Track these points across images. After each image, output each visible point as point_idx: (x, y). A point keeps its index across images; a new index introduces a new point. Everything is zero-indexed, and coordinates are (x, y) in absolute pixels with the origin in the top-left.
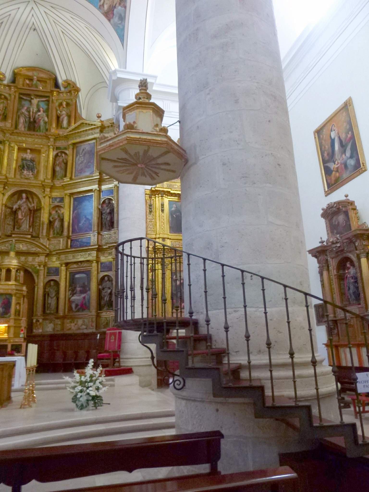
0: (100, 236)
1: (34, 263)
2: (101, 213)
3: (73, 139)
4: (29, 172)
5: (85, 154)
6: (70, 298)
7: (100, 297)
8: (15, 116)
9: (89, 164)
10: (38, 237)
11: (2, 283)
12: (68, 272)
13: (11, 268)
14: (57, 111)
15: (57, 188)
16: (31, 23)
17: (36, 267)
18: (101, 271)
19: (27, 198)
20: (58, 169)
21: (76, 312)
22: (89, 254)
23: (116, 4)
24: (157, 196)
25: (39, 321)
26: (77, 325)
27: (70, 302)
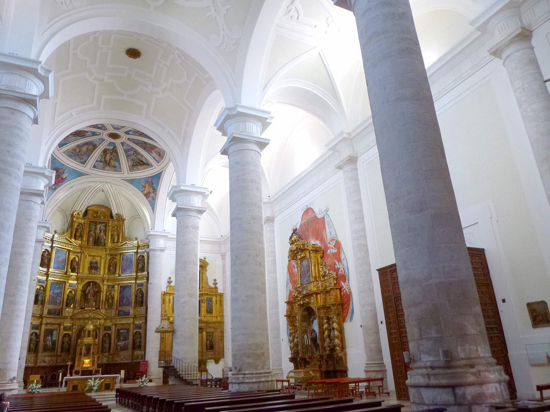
1: (97, 324)
2: (136, 297)
5: (127, 260)
7: (134, 344)
10: (98, 308)
12: (116, 329)
14: (111, 232)
20: (111, 268)
21: (120, 351)
22: (129, 320)
27: (117, 346)
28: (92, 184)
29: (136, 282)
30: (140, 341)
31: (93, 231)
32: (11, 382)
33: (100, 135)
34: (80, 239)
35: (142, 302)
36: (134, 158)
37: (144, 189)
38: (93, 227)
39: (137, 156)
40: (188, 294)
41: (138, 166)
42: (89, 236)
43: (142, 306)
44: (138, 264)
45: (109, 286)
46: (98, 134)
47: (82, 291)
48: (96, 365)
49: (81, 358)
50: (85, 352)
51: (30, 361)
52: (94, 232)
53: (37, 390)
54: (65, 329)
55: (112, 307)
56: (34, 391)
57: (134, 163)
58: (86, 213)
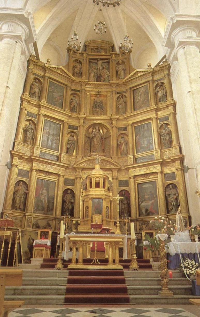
4: (100, 110)
5: (140, 95)
8: (87, 74)
26: (148, 227)
35: (171, 142)
45: (119, 129)
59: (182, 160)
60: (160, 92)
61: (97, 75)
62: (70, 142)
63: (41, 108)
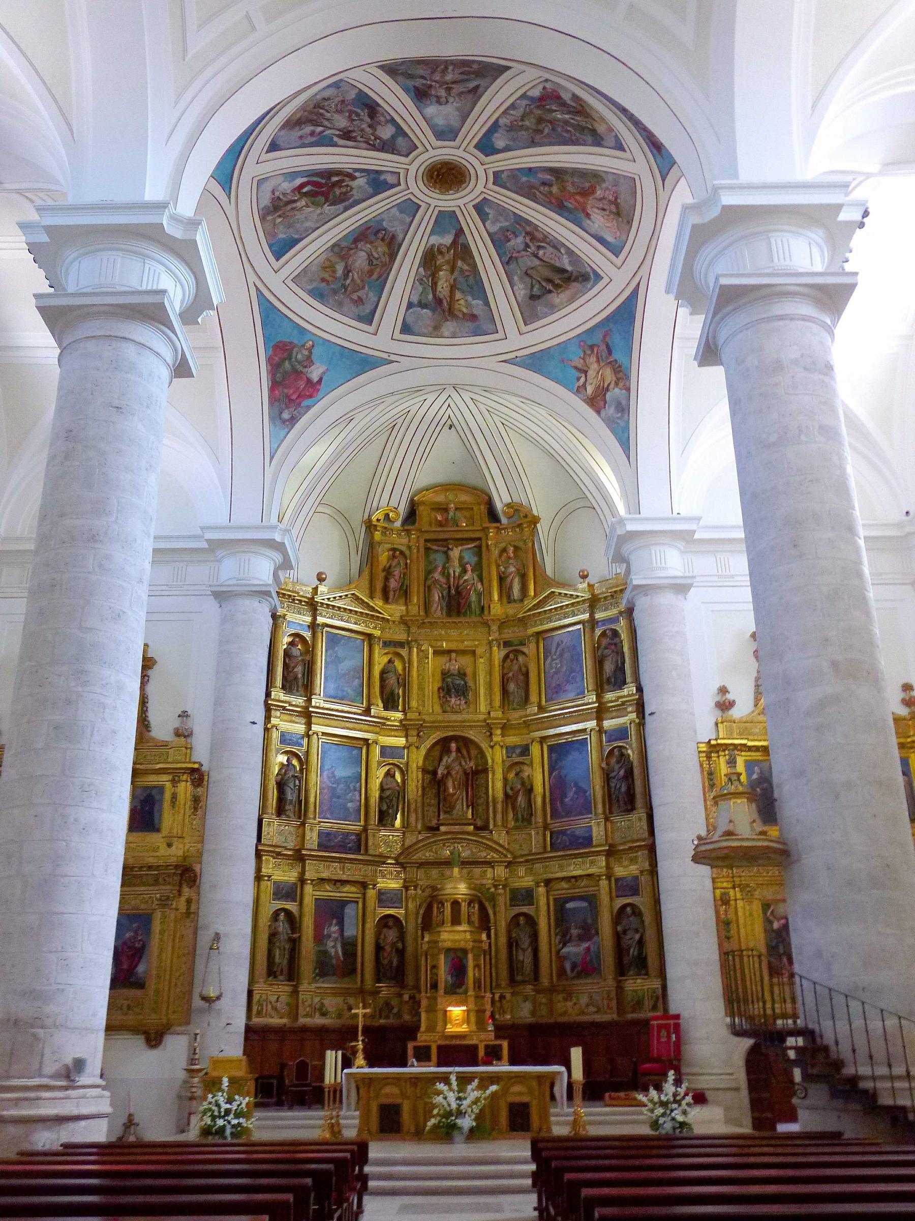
0: (609, 824)
1: (484, 882)
2: (607, 777)
3: (534, 626)
5: (561, 655)
6: (560, 950)
7: (620, 950)
9: (574, 674)
10: (485, 827)
11: (448, 929)
12: (551, 898)
13: (460, 900)
14: (498, 566)
15: (513, 727)
16: (446, 416)
17: (489, 889)
18: (617, 897)
19: (458, 750)
20: (512, 687)
21: (573, 978)
22: (592, 863)
23: (609, 385)
24: (721, 753)
25: (504, 997)
26: (578, 1006)
27: (561, 959)
28: (412, 403)
29: (600, 724)
30: (641, 938)
31: (440, 569)
32: (63, 1083)
33: (399, 184)
34: (402, 600)
36: (530, 264)
37: (583, 380)
38: (439, 559)
39: (541, 253)
40: (835, 665)
41: (549, 296)
42: (429, 587)
43: (633, 809)
44: (599, 663)
45: (510, 749)
46: (391, 179)
47: (424, 771)
48: (491, 1028)
49: (435, 999)
50: (449, 978)
51: (275, 1009)
52: (443, 573)
53: (235, 1122)
54: (383, 898)
55: (530, 822)
56: (220, 1122)
57: (532, 287)
58: (412, 515)
59: (652, 850)
60: (610, 658)
61: (449, 591)
62: (388, 793)
63: (314, 720)
